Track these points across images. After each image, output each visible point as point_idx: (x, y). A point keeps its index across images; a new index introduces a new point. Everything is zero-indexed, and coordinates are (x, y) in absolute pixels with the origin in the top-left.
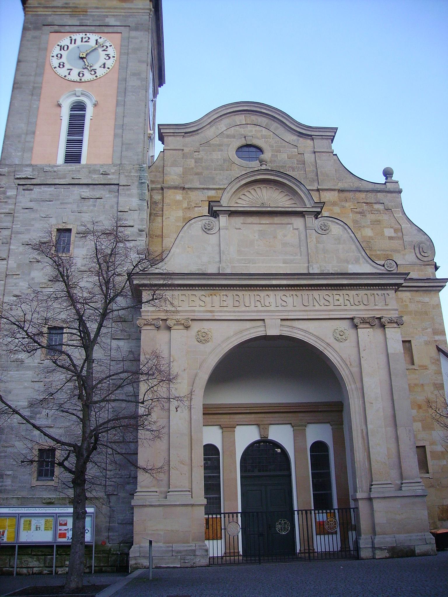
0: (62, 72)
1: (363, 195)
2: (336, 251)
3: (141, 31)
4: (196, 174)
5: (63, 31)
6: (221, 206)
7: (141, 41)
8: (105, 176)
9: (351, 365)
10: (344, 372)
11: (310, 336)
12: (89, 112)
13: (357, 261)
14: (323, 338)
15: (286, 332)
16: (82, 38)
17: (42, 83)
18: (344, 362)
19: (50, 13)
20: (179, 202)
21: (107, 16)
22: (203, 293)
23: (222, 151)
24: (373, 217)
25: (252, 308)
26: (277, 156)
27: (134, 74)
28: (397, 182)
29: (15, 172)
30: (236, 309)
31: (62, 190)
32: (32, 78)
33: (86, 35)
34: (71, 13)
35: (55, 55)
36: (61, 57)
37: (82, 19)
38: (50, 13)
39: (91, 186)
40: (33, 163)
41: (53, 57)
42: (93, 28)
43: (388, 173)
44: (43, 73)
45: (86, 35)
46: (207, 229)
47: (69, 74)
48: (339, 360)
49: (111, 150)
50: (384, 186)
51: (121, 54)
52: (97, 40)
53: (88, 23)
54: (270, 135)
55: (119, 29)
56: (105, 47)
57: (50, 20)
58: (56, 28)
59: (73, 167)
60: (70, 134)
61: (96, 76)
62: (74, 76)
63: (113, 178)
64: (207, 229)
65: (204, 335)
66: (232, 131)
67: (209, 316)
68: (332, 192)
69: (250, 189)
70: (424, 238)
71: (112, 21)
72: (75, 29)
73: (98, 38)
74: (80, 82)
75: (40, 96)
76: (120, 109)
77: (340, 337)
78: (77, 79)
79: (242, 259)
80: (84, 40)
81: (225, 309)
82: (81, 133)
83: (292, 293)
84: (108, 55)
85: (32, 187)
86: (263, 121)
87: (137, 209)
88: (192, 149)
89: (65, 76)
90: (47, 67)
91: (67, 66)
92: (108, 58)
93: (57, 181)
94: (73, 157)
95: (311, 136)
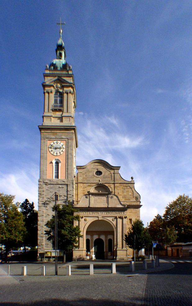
0: (52, 153)
1: (125, 184)
4: (86, 179)
13: (119, 204)
20: (82, 186)
24: (127, 190)
31: (55, 185)
40: (47, 178)
42: (59, 139)
43: (132, 178)
57: (47, 136)
58: (49, 139)
62: (55, 154)
67: (87, 216)
71: (63, 137)
72: (54, 139)
74: (57, 156)
78: (56, 155)
91: (53, 151)
93: (54, 183)
94: (57, 177)
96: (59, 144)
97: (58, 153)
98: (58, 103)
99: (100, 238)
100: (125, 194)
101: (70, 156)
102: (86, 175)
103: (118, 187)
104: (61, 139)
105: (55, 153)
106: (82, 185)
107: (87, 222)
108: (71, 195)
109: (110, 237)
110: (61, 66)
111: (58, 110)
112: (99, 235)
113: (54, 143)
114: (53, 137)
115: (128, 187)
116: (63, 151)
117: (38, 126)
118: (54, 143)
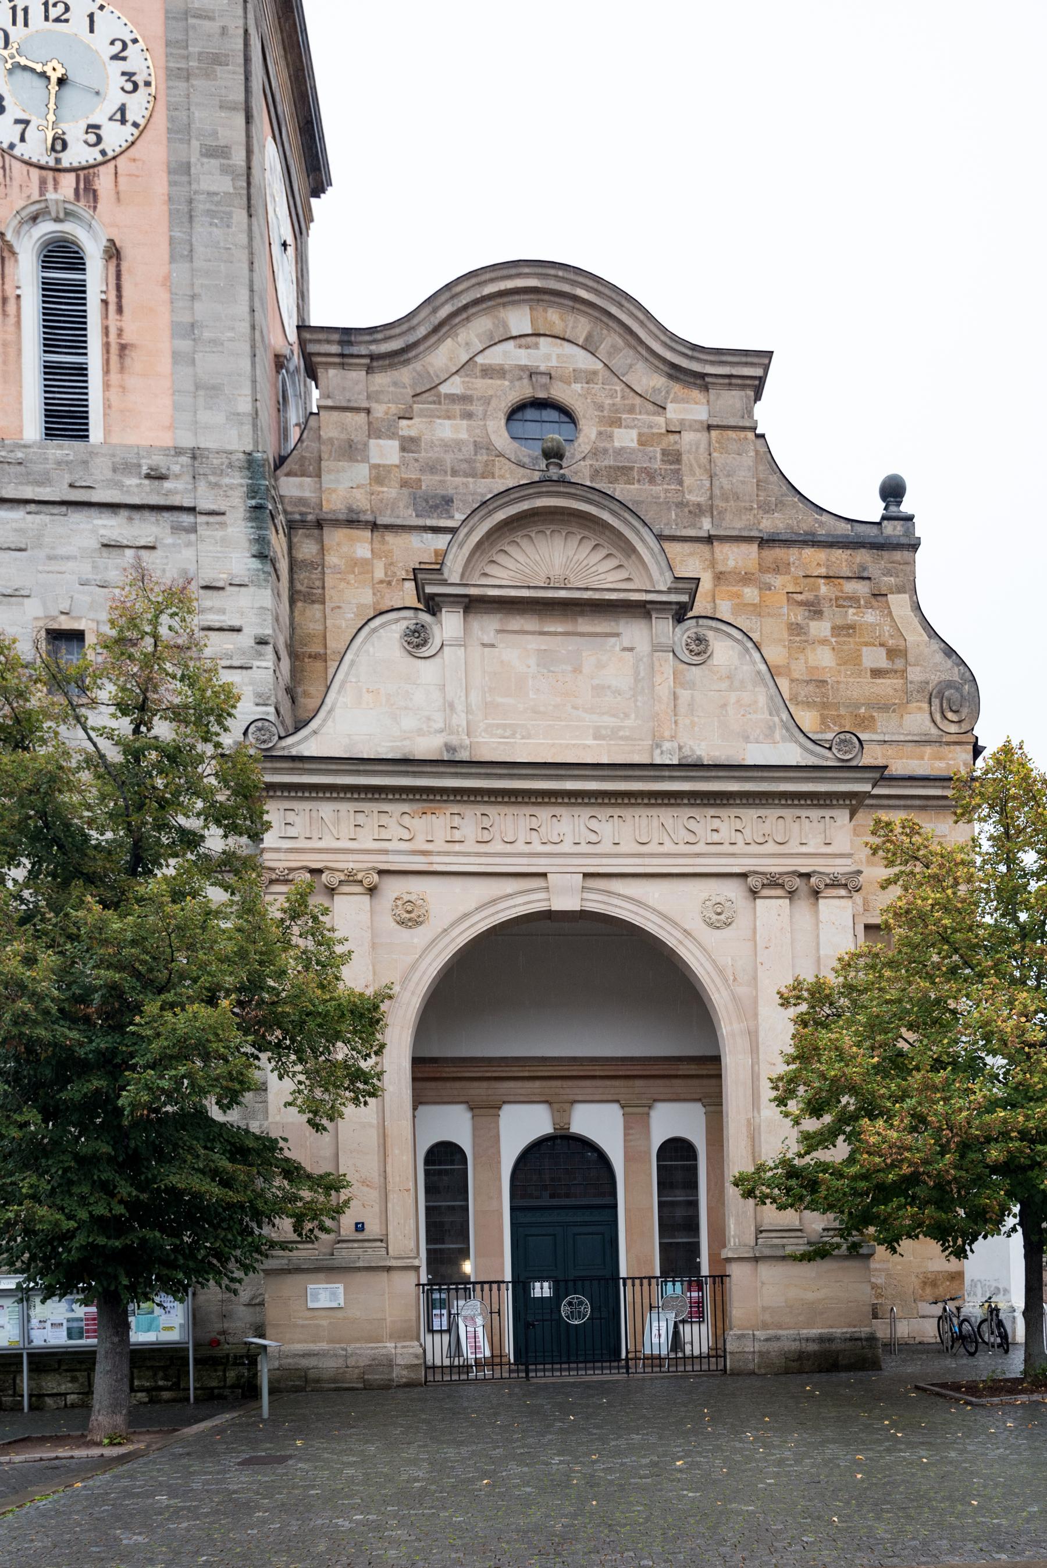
2: (730, 708)
8: (156, 482)
9: (735, 980)
11: (648, 915)
14: (677, 919)
23: (469, 415)
26: (611, 437)
28: (910, 518)
39: (124, 513)
50: (874, 531)
51: (173, 74)
54: (595, 373)
59: (64, 449)
61: (103, 153)
65: (409, 908)
66: (496, 356)
86: (581, 326)
87: (246, 580)
88: (394, 408)
95: (703, 376)
97: (75, 133)
102: (408, 445)
103: (746, 579)
115: (850, 587)
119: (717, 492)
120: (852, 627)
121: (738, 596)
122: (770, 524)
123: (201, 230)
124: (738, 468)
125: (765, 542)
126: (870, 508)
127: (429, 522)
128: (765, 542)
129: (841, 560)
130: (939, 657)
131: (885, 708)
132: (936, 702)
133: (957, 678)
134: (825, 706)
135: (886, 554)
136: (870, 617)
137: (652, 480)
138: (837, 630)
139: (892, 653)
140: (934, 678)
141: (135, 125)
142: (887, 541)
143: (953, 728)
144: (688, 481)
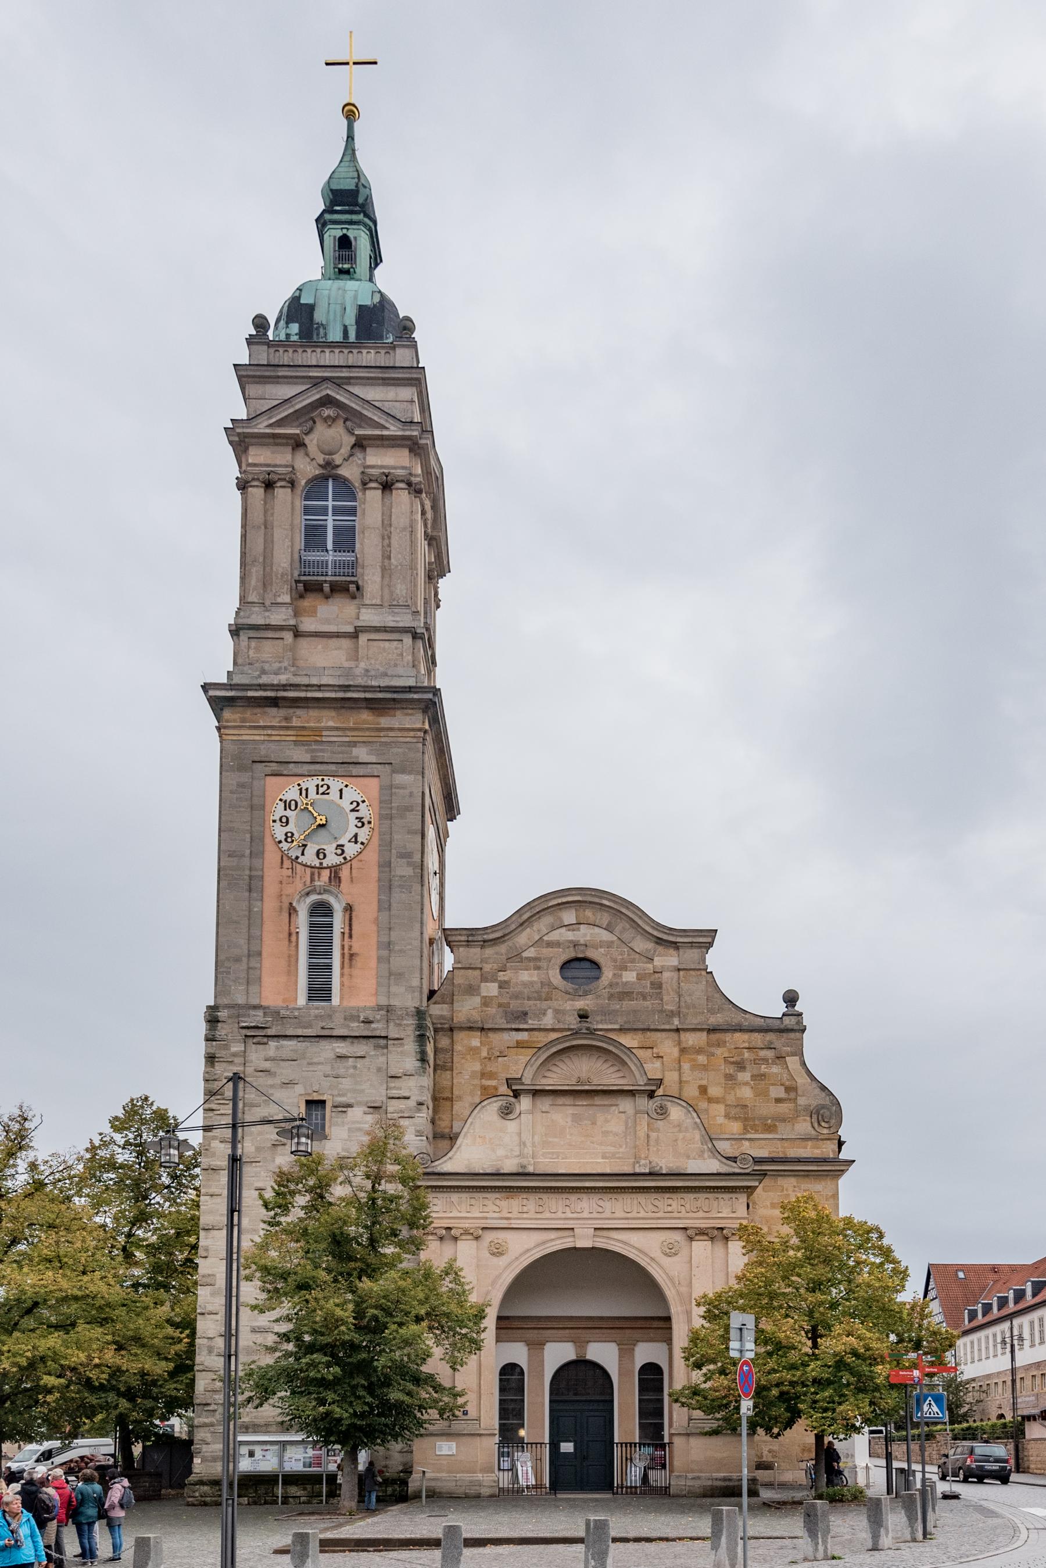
3: (410, 773)
5: (285, 772)
6: (523, 1084)
7: (411, 794)
10: (670, 1293)
12: (338, 921)
15: (601, 1243)
16: (317, 786)
17: (262, 870)
18: (671, 1279)
19: (262, 738)
21: (354, 744)
22: (497, 1195)
25: (560, 1215)
27: (402, 856)
28: (800, 1014)
29: (238, 1016)
30: (539, 1216)
32: (246, 861)
33: (323, 780)
34: (294, 738)
35: (277, 818)
36: (287, 823)
37: (313, 751)
38: (262, 738)
41: (274, 821)
42: (333, 767)
44: (263, 853)
45: (323, 780)
46: (506, 1112)
47: (303, 854)
48: (665, 1277)
49: (374, 981)
50: (778, 1022)
51: (382, 817)
52: (341, 791)
53: (326, 757)
55: (376, 770)
56: (355, 804)
57: (263, 751)
58: (274, 767)
60: (311, 955)
61: (345, 858)
63: (378, 1028)
64: (506, 1112)
67: (504, 1223)
68: (698, 1034)
69: (563, 1057)
70: (827, 1101)
71: (362, 753)
72: (306, 768)
73: (342, 786)
75: (262, 891)
76: (384, 916)
77: (670, 1252)
79: (549, 1153)
80: (321, 790)
81: (525, 1216)
82: (329, 954)
83: (610, 1196)
84: (359, 819)
85: (265, 1040)
89: (297, 858)
90: (268, 840)
92: (360, 824)
94: (320, 991)
96: (334, 795)
97: (330, 849)
98: (330, 546)
99: (588, 1357)
100: (746, 1093)
101: (403, 870)
103: (700, 1051)
104: (348, 768)
105: (311, 850)
106: (475, 1040)
107: (502, 1261)
108: (412, 1103)
109: (646, 1352)
110: (350, 319)
111: (326, 587)
112: (581, 1344)
113: (304, 792)
114: (300, 754)
115: (763, 1053)
116: (360, 840)
117: (205, 687)
118: (304, 792)
119: (683, 1004)
120: (764, 1075)
121: (694, 1060)
122: (714, 1020)
123: (397, 896)
124: (696, 990)
125: (711, 1031)
126: (778, 1009)
127: (513, 1027)
128: (711, 1031)
129: (758, 1039)
130: (817, 1091)
131: (784, 1120)
132: (815, 1117)
133: (828, 1103)
134: (746, 1119)
135: (785, 1035)
136: (775, 1069)
137: (644, 998)
138: (754, 1077)
139: (788, 1089)
140: (814, 1103)
141: (362, 843)
142: (787, 1028)
143: (825, 1131)
144: (665, 998)
